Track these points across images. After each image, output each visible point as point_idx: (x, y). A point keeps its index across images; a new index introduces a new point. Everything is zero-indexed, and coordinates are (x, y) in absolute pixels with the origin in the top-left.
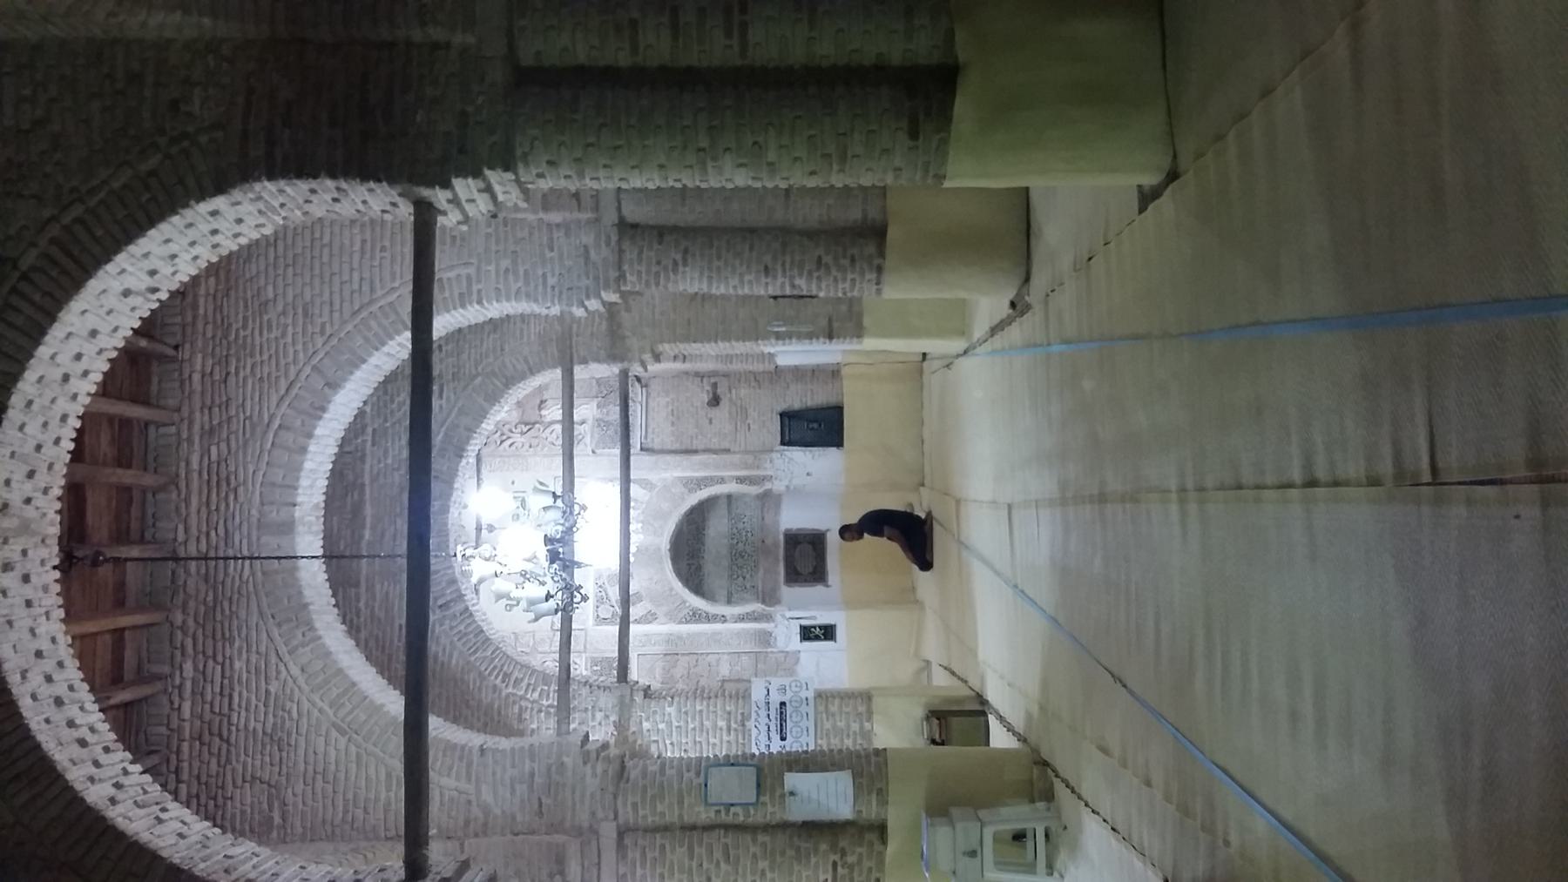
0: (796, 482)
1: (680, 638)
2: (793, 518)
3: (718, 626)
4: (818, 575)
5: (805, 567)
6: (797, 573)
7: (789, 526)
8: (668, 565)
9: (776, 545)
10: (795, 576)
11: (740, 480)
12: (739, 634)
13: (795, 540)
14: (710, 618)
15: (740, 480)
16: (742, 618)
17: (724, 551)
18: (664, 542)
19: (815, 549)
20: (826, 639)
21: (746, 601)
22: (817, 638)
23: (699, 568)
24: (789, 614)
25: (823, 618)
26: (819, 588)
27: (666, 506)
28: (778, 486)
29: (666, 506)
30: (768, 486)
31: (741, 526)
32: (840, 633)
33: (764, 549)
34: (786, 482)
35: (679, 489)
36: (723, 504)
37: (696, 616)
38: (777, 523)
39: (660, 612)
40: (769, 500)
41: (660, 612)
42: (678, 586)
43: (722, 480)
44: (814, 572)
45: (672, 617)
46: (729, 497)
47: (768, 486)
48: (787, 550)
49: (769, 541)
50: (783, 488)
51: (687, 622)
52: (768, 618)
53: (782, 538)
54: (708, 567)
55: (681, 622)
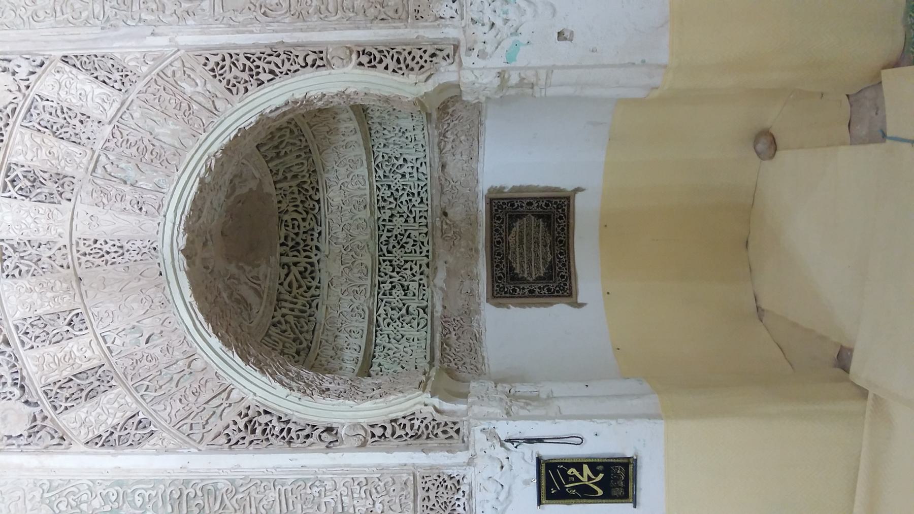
0: (527, 58)
1: (211, 492)
2: (508, 162)
3: (313, 460)
4: (556, 283)
5: (530, 267)
6: (514, 278)
7: (498, 184)
8: (181, 292)
9: (472, 222)
10: (508, 285)
11: (370, 57)
12: (368, 486)
13: (507, 209)
14: (290, 434)
15: (370, 57)
16: (378, 435)
17: (363, 237)
18: (166, 230)
19: (549, 226)
20: (608, 497)
21: (395, 388)
22: (585, 494)
23: (309, 272)
24: (506, 429)
25: (601, 441)
26: (560, 310)
27: (167, 132)
28: (475, 75)
29: (167, 132)
30: (447, 74)
31: (396, 181)
32: (649, 480)
33: (447, 228)
34: (497, 62)
35: (199, 86)
36: (348, 124)
37: (257, 428)
38: (473, 175)
39: (163, 414)
40: (449, 112)
41: (163, 414)
42: (211, 351)
43: (317, 60)
44: (548, 277)
45: (191, 433)
46: (362, 112)
47: (447, 74)
48: (492, 230)
49: (457, 213)
50: (489, 80)
51: (232, 444)
52: (449, 433)
53: (482, 206)
54: (330, 269)
55: (213, 448)
